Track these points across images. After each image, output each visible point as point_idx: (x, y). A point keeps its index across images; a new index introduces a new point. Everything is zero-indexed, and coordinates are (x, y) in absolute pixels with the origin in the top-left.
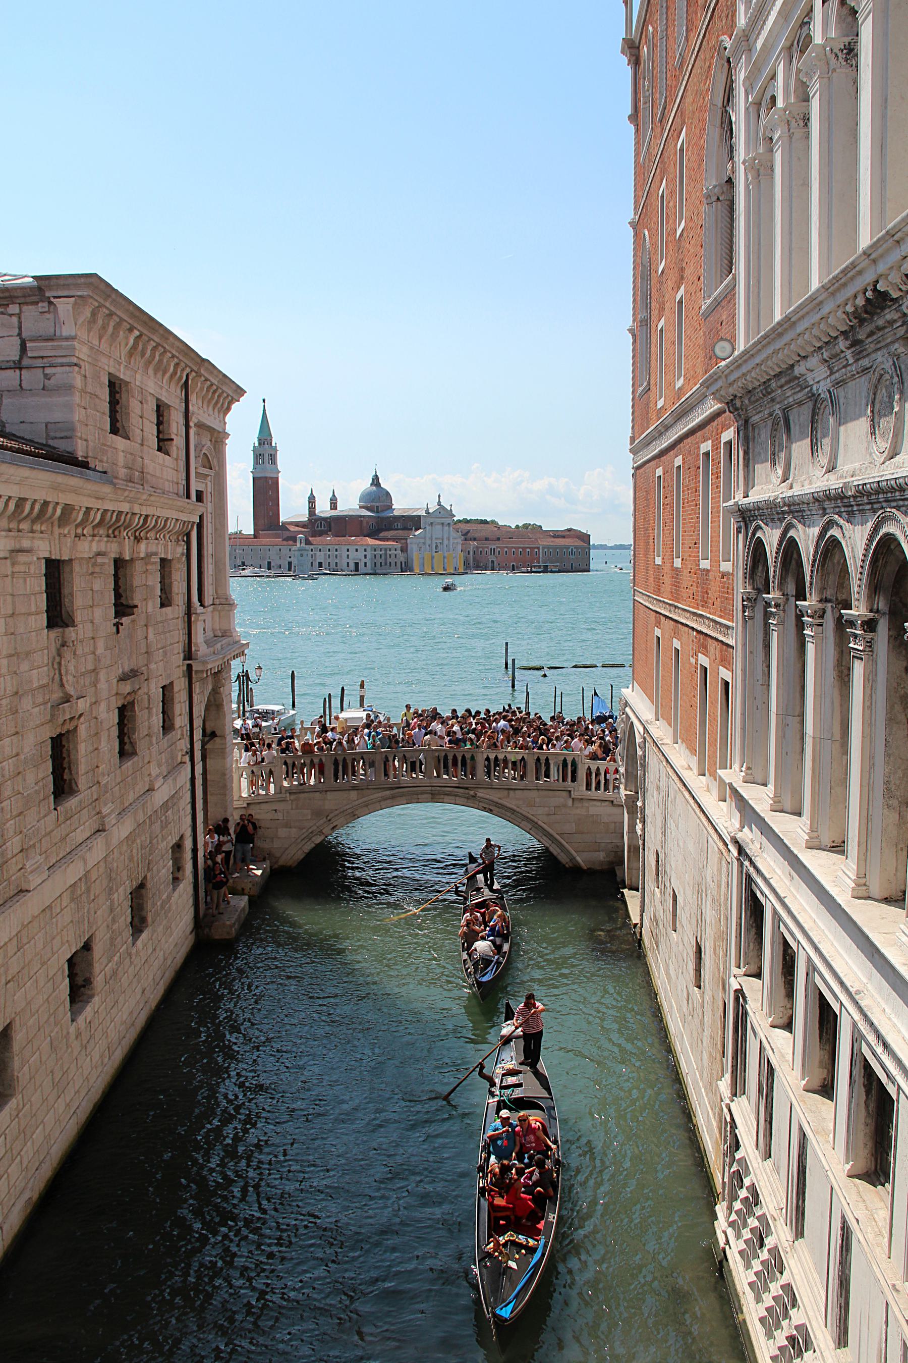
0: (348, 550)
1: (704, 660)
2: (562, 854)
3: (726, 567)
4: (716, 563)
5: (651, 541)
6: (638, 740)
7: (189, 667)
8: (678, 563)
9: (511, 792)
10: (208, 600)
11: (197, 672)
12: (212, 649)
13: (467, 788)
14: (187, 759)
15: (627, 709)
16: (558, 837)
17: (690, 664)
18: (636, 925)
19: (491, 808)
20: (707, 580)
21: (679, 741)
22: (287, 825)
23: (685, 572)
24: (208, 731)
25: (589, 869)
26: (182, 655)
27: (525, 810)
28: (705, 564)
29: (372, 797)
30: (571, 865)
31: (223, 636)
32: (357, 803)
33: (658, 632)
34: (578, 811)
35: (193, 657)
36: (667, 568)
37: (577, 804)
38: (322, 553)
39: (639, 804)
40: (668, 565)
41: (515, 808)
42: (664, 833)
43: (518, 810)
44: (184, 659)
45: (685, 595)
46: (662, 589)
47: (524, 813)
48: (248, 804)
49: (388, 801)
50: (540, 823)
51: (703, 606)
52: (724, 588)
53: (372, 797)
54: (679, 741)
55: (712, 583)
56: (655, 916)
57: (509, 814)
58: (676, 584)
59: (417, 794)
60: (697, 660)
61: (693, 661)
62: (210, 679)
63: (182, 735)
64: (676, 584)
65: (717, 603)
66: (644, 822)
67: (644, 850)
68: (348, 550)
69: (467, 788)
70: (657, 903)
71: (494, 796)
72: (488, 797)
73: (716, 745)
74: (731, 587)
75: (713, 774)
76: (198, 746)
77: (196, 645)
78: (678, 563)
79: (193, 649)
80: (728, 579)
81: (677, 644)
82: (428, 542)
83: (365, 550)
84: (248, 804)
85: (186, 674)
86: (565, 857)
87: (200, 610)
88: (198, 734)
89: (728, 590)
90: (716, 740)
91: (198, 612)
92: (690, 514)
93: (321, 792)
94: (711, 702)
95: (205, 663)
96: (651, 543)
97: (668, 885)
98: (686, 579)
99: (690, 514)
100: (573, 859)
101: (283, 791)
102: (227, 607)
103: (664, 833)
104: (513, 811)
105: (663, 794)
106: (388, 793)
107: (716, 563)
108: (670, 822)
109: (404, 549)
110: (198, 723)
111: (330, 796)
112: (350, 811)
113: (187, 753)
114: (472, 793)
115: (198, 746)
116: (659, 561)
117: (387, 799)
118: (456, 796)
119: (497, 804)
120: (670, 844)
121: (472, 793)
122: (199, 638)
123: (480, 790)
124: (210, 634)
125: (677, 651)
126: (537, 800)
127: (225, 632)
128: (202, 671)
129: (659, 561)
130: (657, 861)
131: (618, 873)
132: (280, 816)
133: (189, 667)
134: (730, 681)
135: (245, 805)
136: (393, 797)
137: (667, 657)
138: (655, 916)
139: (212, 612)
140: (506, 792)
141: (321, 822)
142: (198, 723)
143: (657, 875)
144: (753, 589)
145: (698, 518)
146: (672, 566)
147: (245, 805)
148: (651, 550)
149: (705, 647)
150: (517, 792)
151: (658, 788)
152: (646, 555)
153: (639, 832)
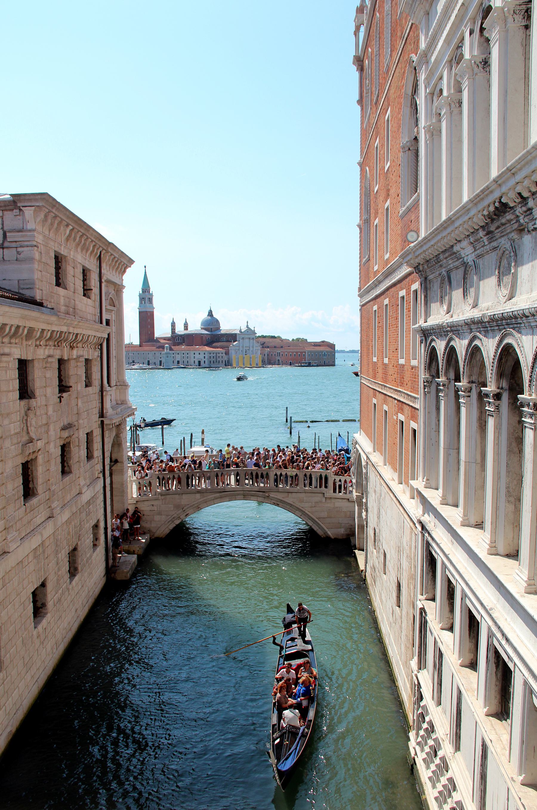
0: (194, 354)
1: (401, 417)
2: (319, 530)
3: (414, 363)
4: (408, 360)
5: (371, 348)
6: (364, 463)
7: (102, 422)
8: (386, 361)
9: (290, 494)
10: (113, 383)
11: (107, 425)
12: (115, 412)
13: (264, 492)
14: (101, 475)
16: (317, 520)
17: (394, 419)
18: (362, 571)
19: (278, 503)
20: (403, 370)
21: (387, 464)
22: (160, 514)
23: (391, 366)
24: (113, 459)
25: (335, 538)
26: (98, 415)
27: (298, 505)
28: (402, 361)
29: (209, 497)
30: (325, 536)
31: (122, 404)
32: (200, 500)
33: (375, 401)
34: (329, 505)
35: (105, 416)
36: (380, 364)
37: (328, 501)
38: (179, 355)
39: (364, 500)
40: (380, 361)
41: (292, 503)
42: (379, 518)
43: (294, 504)
44: (99, 417)
45: (390, 380)
46: (377, 376)
47: (297, 506)
48: (137, 501)
49: (218, 499)
50: (306, 512)
51: (401, 386)
52: (413, 375)
53: (209, 497)
54: (387, 464)
55: (406, 373)
56: (373, 566)
57: (288, 507)
58: (385, 373)
59: (235, 495)
60: (397, 417)
61: (395, 417)
62: (114, 429)
63: (99, 461)
64: (385, 373)
65: (409, 384)
66: (367, 511)
67: (367, 527)
68: (194, 354)
69: (264, 492)
70: (375, 558)
71: (280, 496)
72: (276, 497)
73: (409, 467)
74: (417, 375)
75: (407, 483)
76: (107, 468)
77: (106, 409)
78: (386, 361)
79: (105, 411)
80: (415, 370)
81: (385, 408)
82: (241, 349)
83: (204, 354)
84: (137, 501)
85: (101, 426)
86: (321, 531)
87: (108, 388)
88: (107, 461)
89: (415, 376)
90: (409, 463)
91: (107, 390)
92: (393, 332)
93: (179, 494)
94: (406, 442)
95: (111, 419)
96: (371, 349)
97: (381, 547)
98: (391, 370)
99: (393, 332)
100: (325, 533)
101: (157, 494)
102: (124, 387)
103: (379, 518)
104: (291, 505)
105: (378, 495)
106: (218, 495)
107: (408, 360)
108: (382, 511)
109: (227, 353)
110: (107, 454)
111: (184, 496)
112: (196, 505)
113: (101, 472)
114: (267, 494)
115: (107, 468)
116: (375, 359)
117: (217, 499)
118: (258, 496)
119: (281, 501)
120: (382, 523)
121: (267, 494)
122: (108, 405)
123: (272, 493)
124: (114, 403)
125: (386, 412)
126: (305, 498)
127: (123, 401)
128: (110, 424)
129: (375, 359)
130: (375, 534)
131: (352, 540)
133: (102, 422)
134: (416, 429)
135: (135, 502)
136: (221, 497)
137: (380, 416)
138: (373, 566)
139: (115, 390)
140: (286, 494)
141: (180, 512)
142: (107, 454)
143: (375, 542)
144: (430, 375)
145: (398, 334)
146: (383, 362)
147: (135, 502)
148: (371, 353)
149: (402, 410)
150: (293, 494)
151: (375, 491)
152: (368, 355)
153: (364, 517)
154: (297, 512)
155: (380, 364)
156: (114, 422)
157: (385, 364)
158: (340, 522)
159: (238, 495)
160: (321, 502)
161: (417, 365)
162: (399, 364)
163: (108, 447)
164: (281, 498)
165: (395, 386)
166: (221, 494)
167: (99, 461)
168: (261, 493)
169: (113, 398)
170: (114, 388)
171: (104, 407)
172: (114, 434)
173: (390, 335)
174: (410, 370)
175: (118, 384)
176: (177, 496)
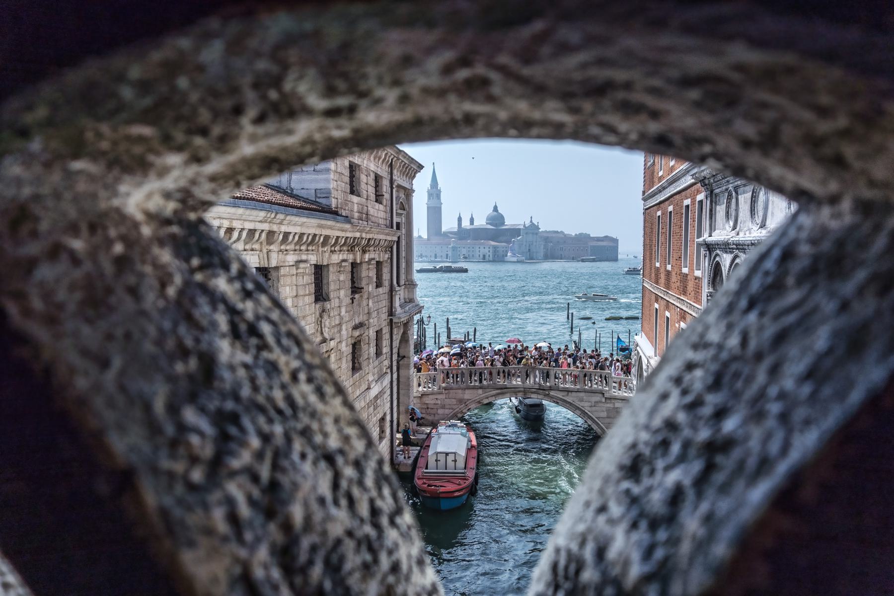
2: (599, 429)
3: (698, 273)
4: (691, 270)
5: (654, 253)
7: (391, 320)
8: (669, 267)
9: (570, 394)
10: (402, 282)
11: (395, 323)
12: (403, 310)
14: (389, 371)
15: (638, 348)
16: (596, 420)
17: (675, 327)
19: (558, 401)
20: (686, 279)
22: (443, 407)
23: (674, 274)
24: (401, 355)
26: (387, 314)
27: (578, 403)
28: (685, 270)
31: (409, 302)
32: (482, 396)
33: (656, 306)
35: (393, 315)
41: (572, 402)
43: (573, 403)
44: (388, 316)
45: (673, 287)
46: (660, 282)
48: (422, 395)
51: (683, 294)
52: (696, 285)
53: (491, 393)
57: (568, 405)
60: (680, 325)
62: (402, 326)
63: (387, 357)
71: (560, 395)
72: (556, 395)
74: (700, 286)
76: (395, 363)
79: (393, 310)
80: (699, 281)
81: (667, 314)
84: (422, 395)
85: (389, 324)
87: (397, 288)
88: (395, 357)
91: (397, 290)
92: (677, 240)
95: (400, 318)
96: (653, 254)
98: (674, 278)
99: (677, 240)
101: (441, 388)
104: (570, 404)
107: (691, 270)
110: (395, 351)
111: (467, 391)
112: (478, 400)
113: (389, 367)
114: (547, 392)
115: (395, 363)
116: (658, 265)
118: (538, 394)
121: (547, 392)
122: (397, 303)
124: (403, 301)
125: (668, 318)
126: (584, 397)
127: (411, 299)
128: (398, 323)
133: (391, 320)
135: (420, 395)
137: (661, 323)
139: (404, 289)
140: (566, 393)
141: (462, 406)
142: (395, 351)
145: (681, 243)
146: (666, 269)
147: (420, 395)
149: (685, 319)
150: (573, 393)
152: (651, 259)
154: (577, 411)
155: (662, 270)
156: (402, 320)
157: (668, 271)
161: (701, 276)
162: (682, 273)
163: (396, 344)
165: (678, 295)
166: (502, 391)
167: (387, 357)
168: (542, 391)
169: (402, 297)
170: (403, 287)
171: (394, 306)
172: (402, 331)
173: (674, 243)
174: (693, 280)
175: (407, 283)
176: (460, 391)
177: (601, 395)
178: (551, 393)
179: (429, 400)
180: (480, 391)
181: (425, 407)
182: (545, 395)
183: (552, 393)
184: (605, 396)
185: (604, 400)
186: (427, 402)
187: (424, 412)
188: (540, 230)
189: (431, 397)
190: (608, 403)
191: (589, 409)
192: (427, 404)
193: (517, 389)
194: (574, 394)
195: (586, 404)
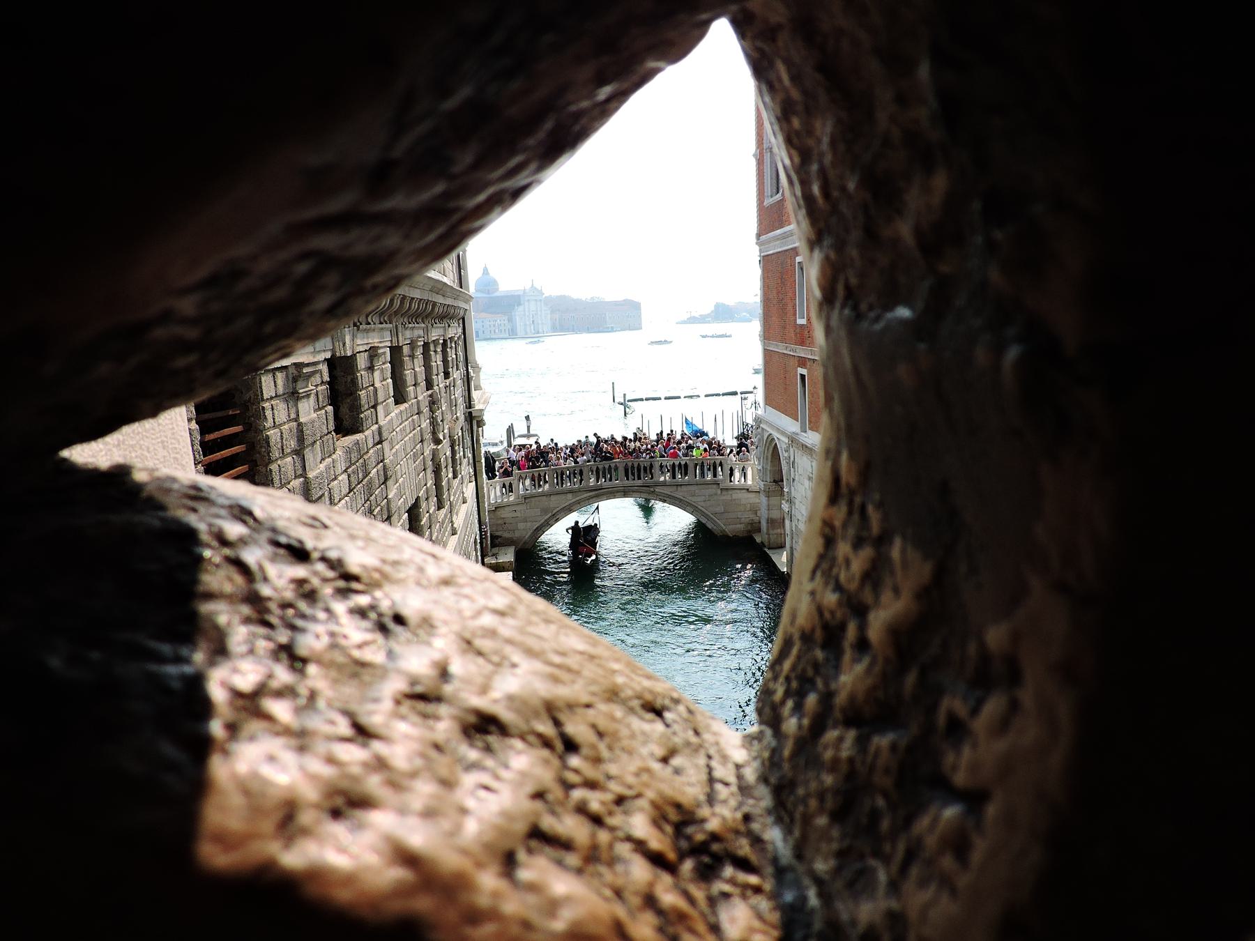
9: (679, 488)
13: (648, 486)
16: (712, 516)
22: (525, 520)
29: (582, 497)
30: (721, 534)
34: (724, 498)
37: (724, 493)
41: (682, 498)
43: (684, 499)
49: (594, 499)
50: (699, 507)
59: (614, 493)
69: (648, 486)
106: (594, 493)
111: (553, 498)
114: (652, 489)
118: (641, 492)
119: (669, 496)
121: (652, 489)
132: (518, 514)
135: (494, 509)
147: (494, 509)
150: (683, 487)
158: (739, 517)
159: (618, 492)
160: (716, 494)
164: (669, 493)
166: (596, 492)
177: (715, 486)
178: (657, 490)
179: (505, 514)
180: (570, 496)
181: (500, 522)
182: (649, 494)
183: (657, 490)
184: (721, 487)
185: (719, 492)
186: (502, 516)
187: (501, 529)
188: (544, 296)
189: (506, 509)
190: (724, 495)
191: (702, 504)
192: (503, 518)
193: (602, 491)
194: (684, 488)
195: (699, 499)
